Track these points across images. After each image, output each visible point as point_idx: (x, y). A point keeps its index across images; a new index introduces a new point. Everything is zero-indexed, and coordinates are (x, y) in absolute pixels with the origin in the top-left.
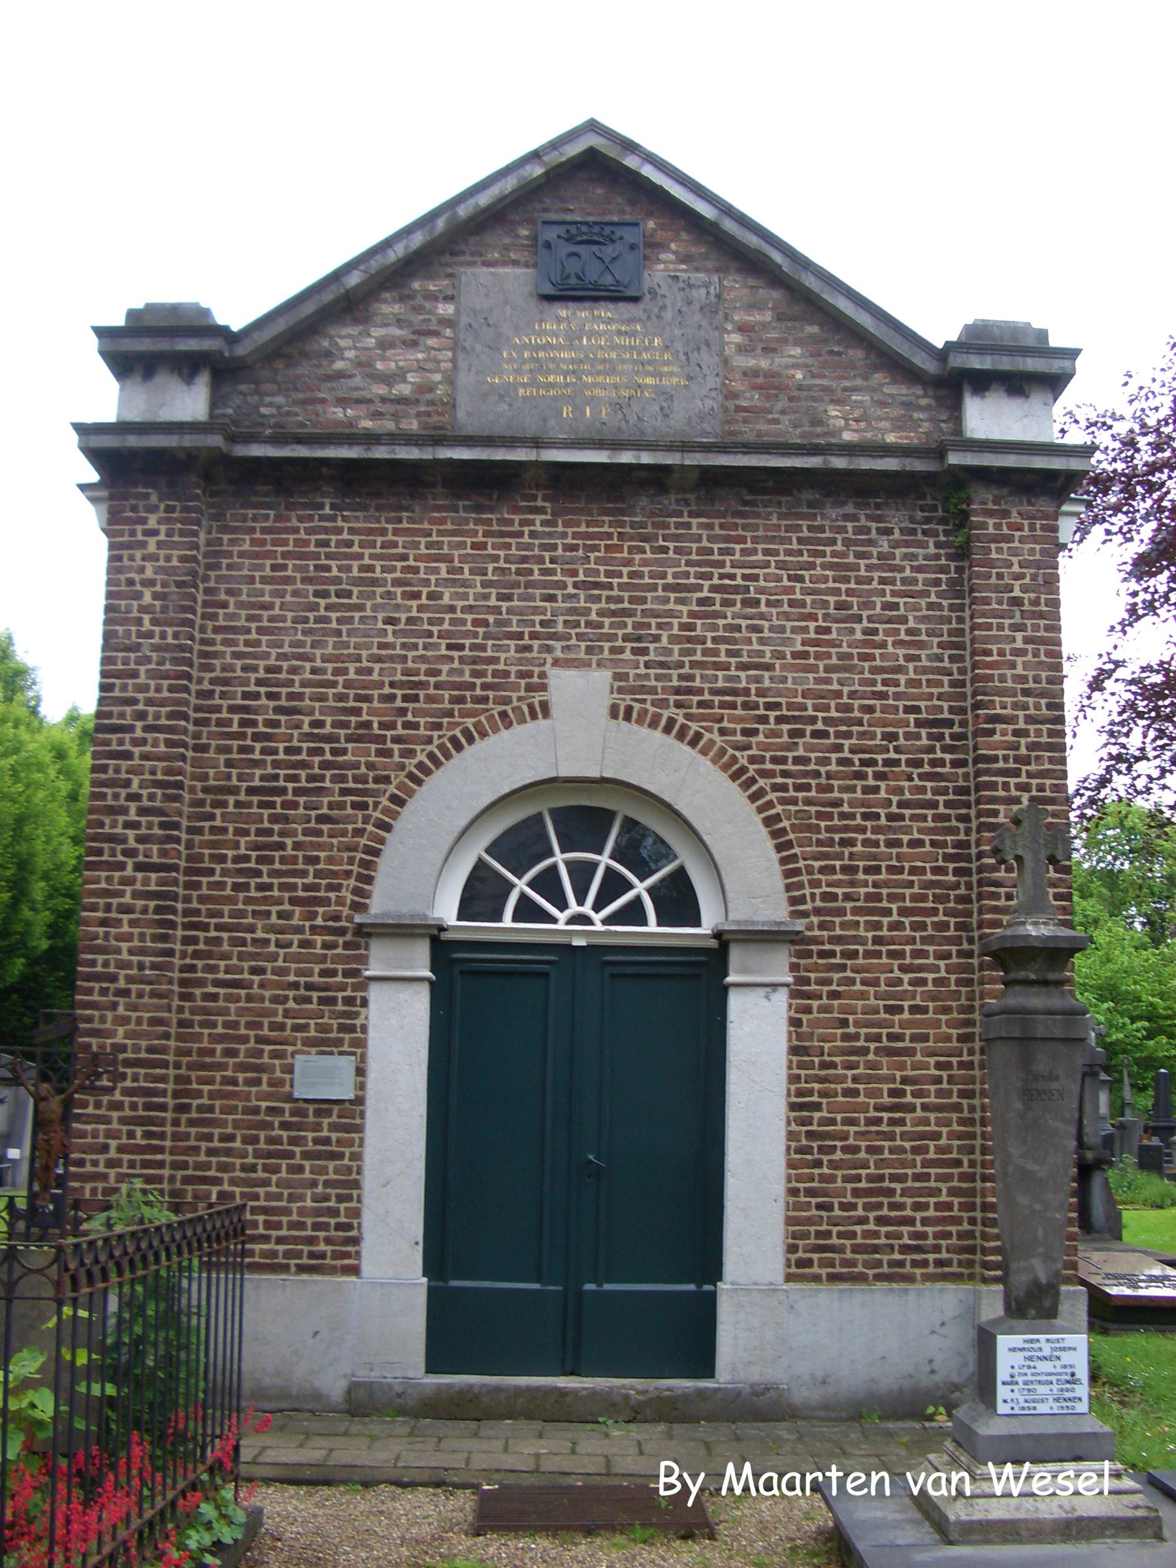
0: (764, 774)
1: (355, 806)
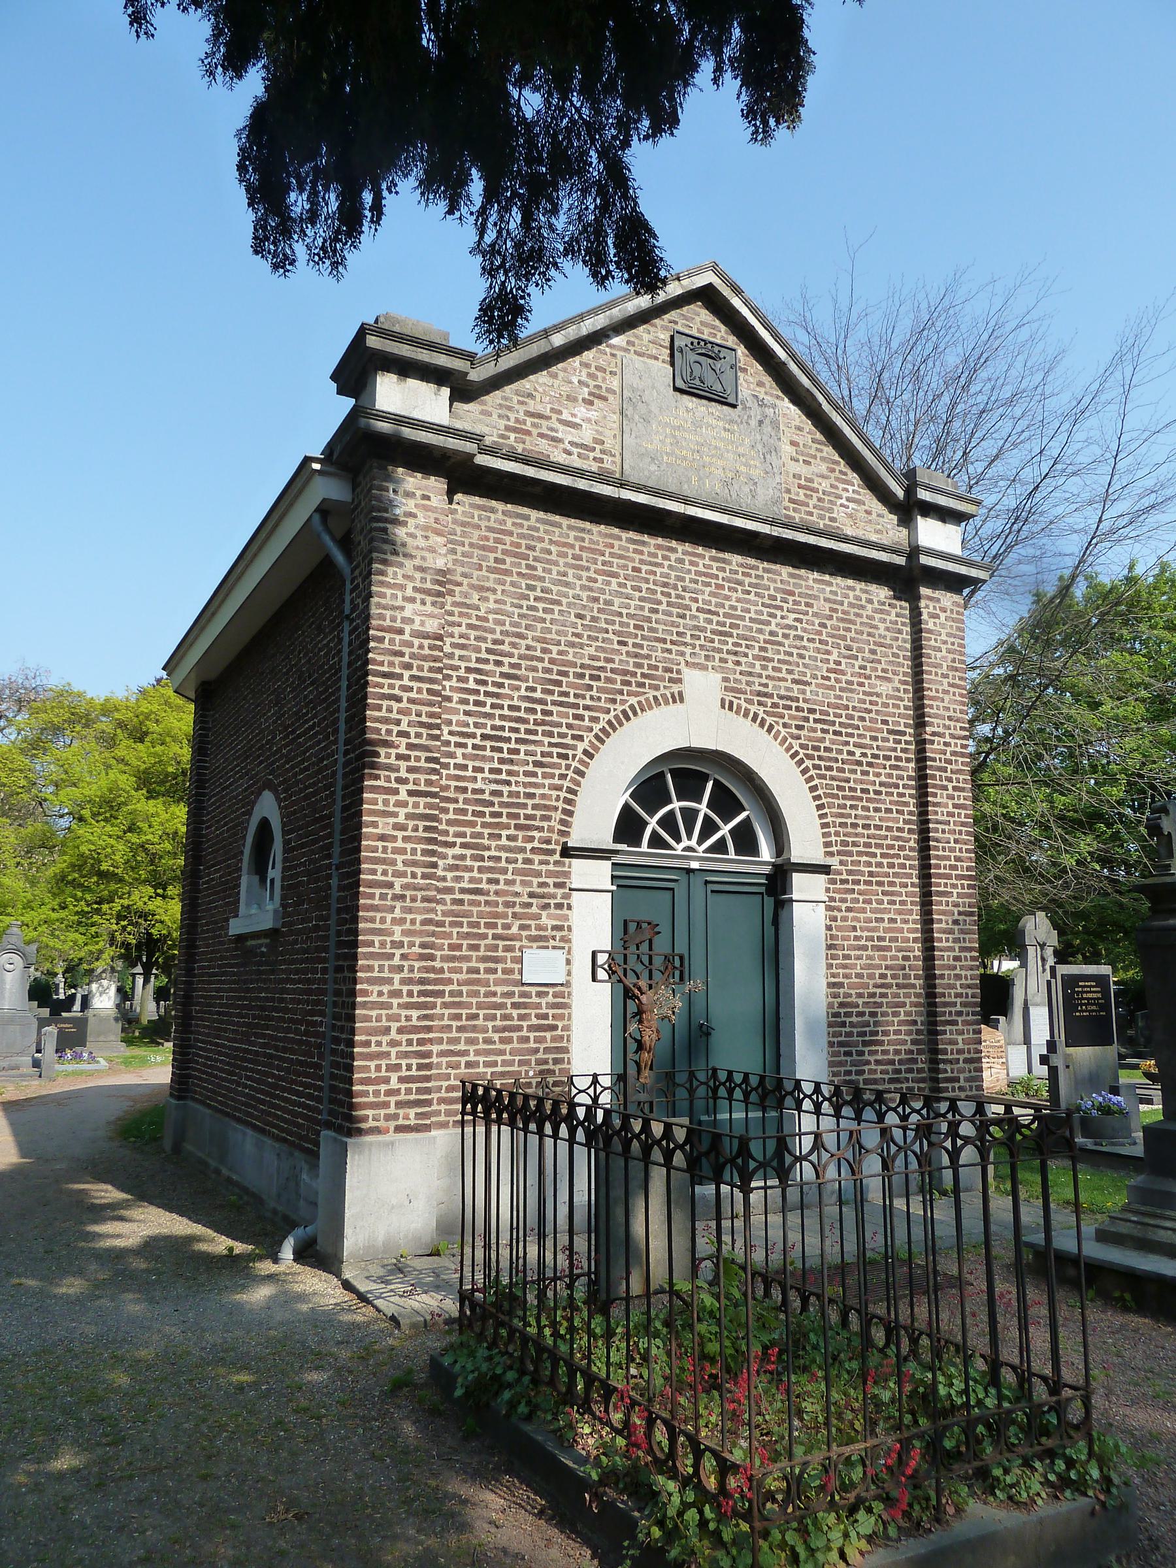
1: (560, 756)
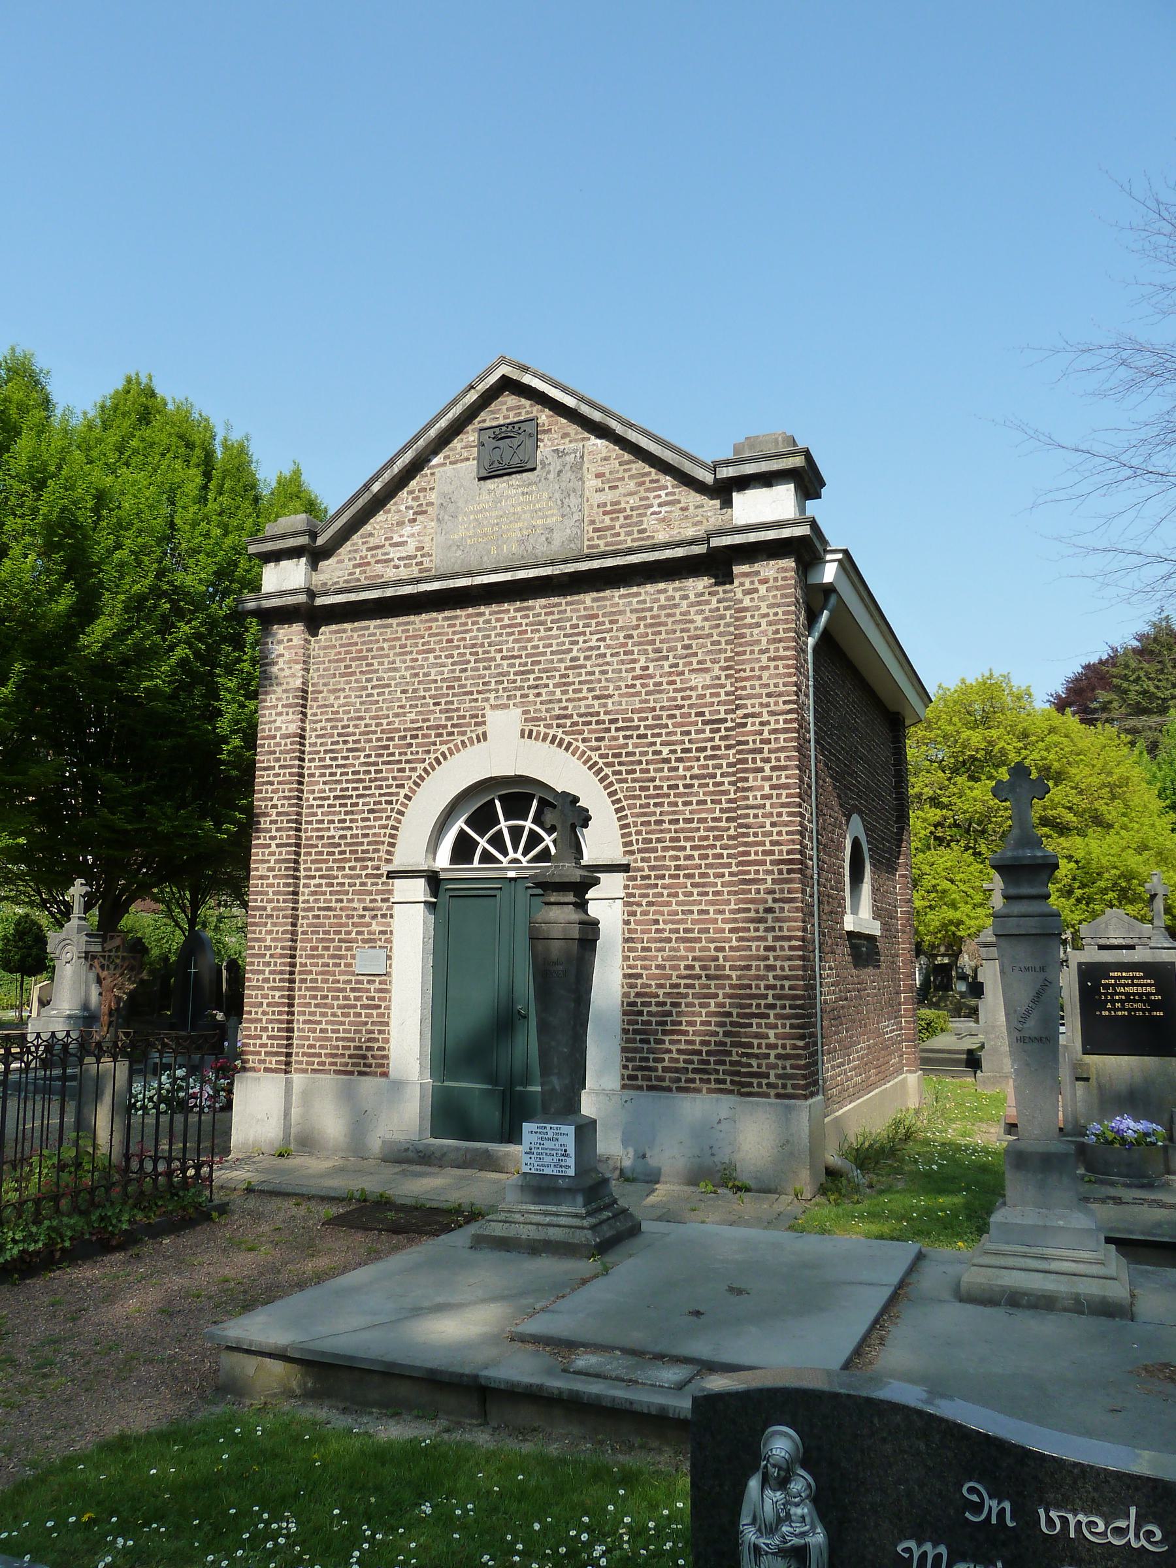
0: (607, 765)
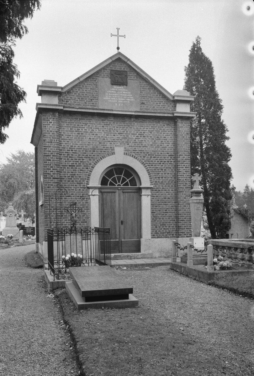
0: (146, 163)
